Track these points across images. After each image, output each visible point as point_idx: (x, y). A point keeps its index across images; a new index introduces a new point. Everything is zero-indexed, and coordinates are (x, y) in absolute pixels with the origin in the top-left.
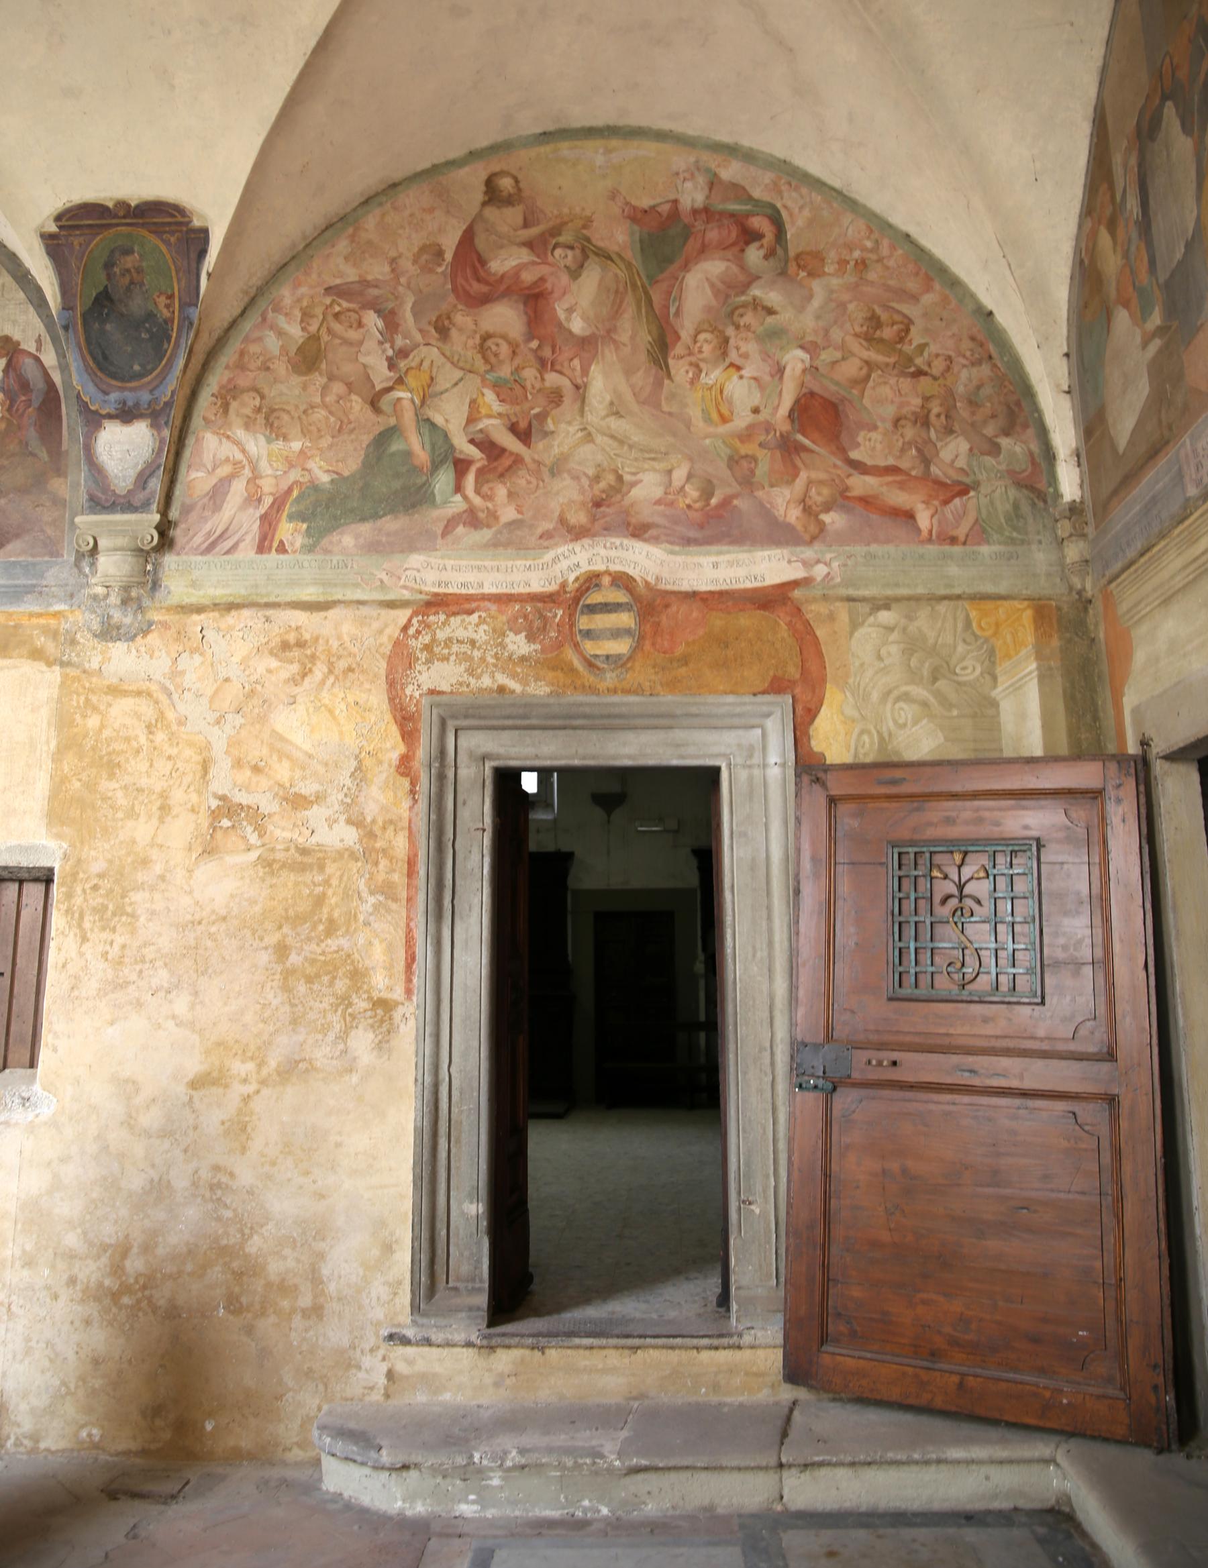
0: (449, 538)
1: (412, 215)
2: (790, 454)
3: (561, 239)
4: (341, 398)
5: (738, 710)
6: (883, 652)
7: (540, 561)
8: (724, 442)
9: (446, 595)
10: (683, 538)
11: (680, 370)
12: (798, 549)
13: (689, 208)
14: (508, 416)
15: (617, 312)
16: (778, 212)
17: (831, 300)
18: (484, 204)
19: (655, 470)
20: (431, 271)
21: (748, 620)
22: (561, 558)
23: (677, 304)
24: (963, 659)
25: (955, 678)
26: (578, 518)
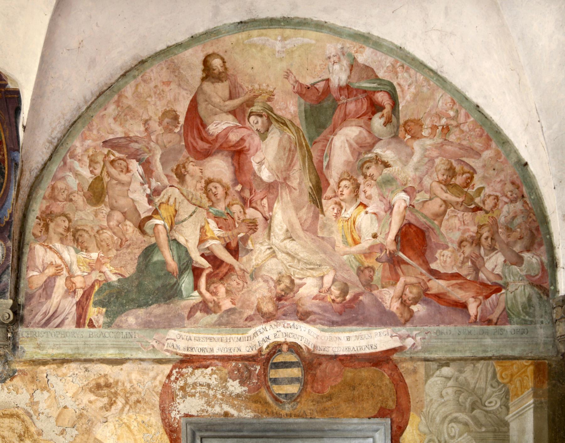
0: (192, 320)
1: (156, 87)
2: (394, 266)
3: (254, 109)
4: (120, 223)
5: (360, 427)
6: (444, 393)
7: (247, 335)
8: (355, 258)
9: (192, 356)
10: (329, 321)
11: (329, 206)
12: (397, 328)
13: (336, 86)
14: (224, 238)
15: (290, 165)
16: (394, 89)
17: (425, 157)
18: (203, 79)
19: (314, 277)
20: (171, 131)
21: (366, 373)
22: (259, 333)
23: (328, 159)
24: (490, 397)
25: (485, 408)
26: (268, 307)
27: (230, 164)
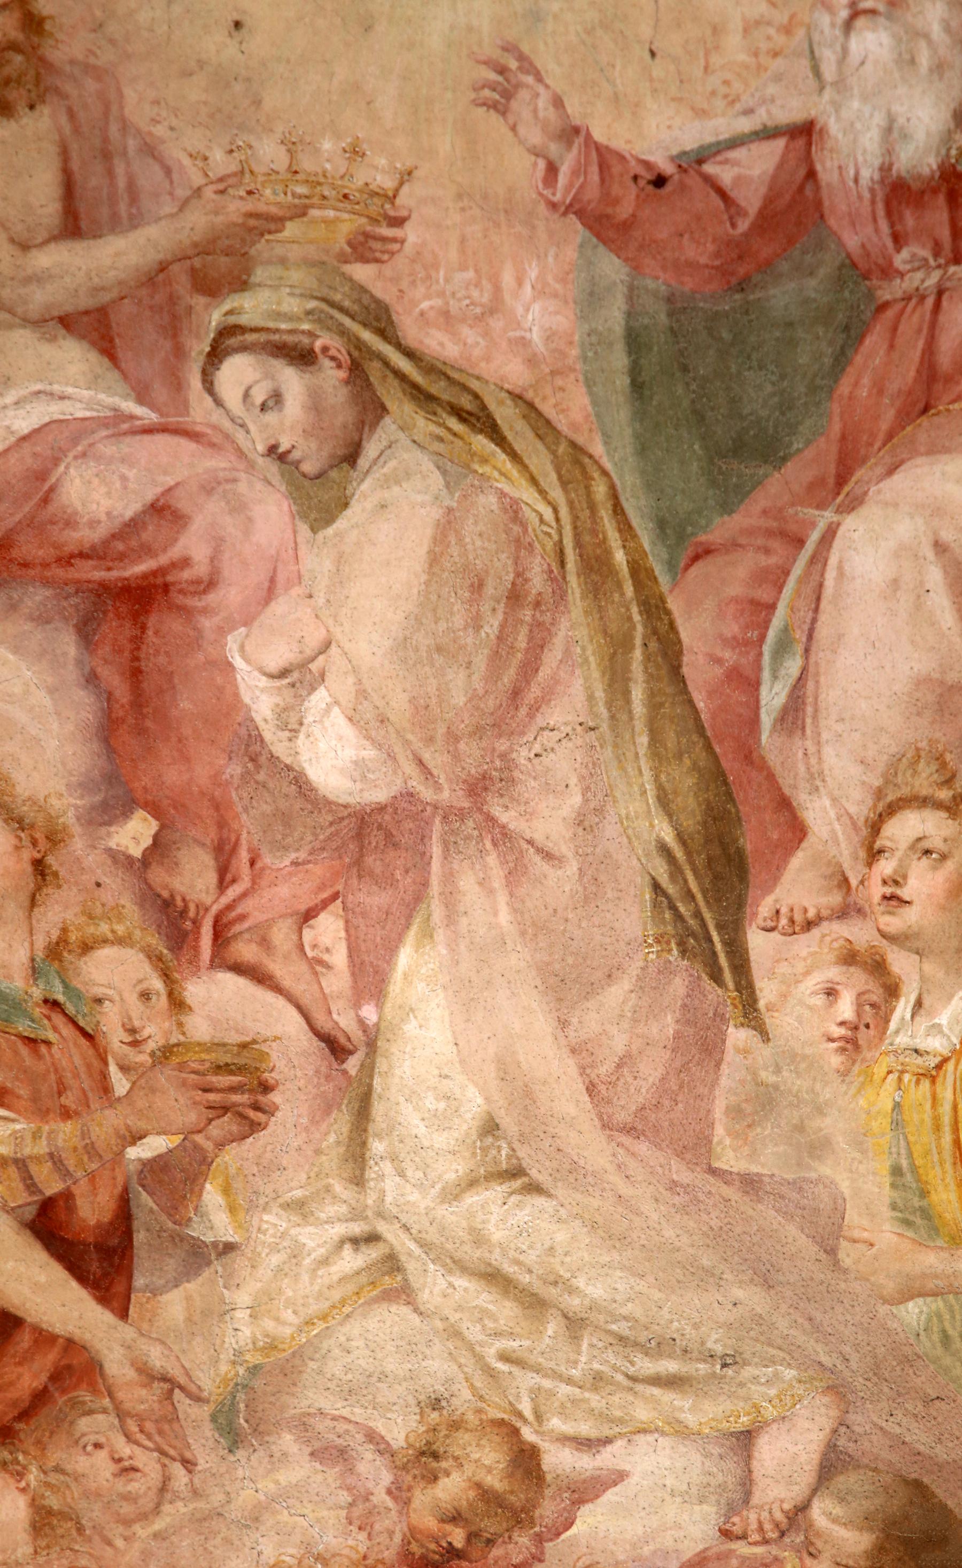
27: (71, 673)
